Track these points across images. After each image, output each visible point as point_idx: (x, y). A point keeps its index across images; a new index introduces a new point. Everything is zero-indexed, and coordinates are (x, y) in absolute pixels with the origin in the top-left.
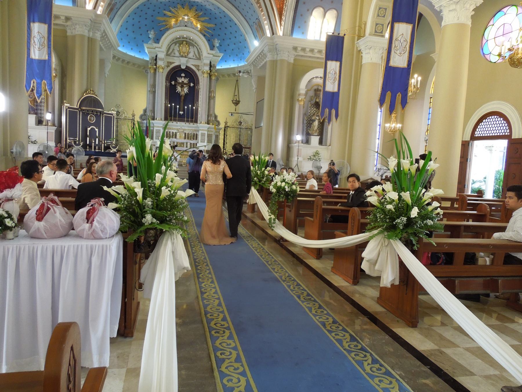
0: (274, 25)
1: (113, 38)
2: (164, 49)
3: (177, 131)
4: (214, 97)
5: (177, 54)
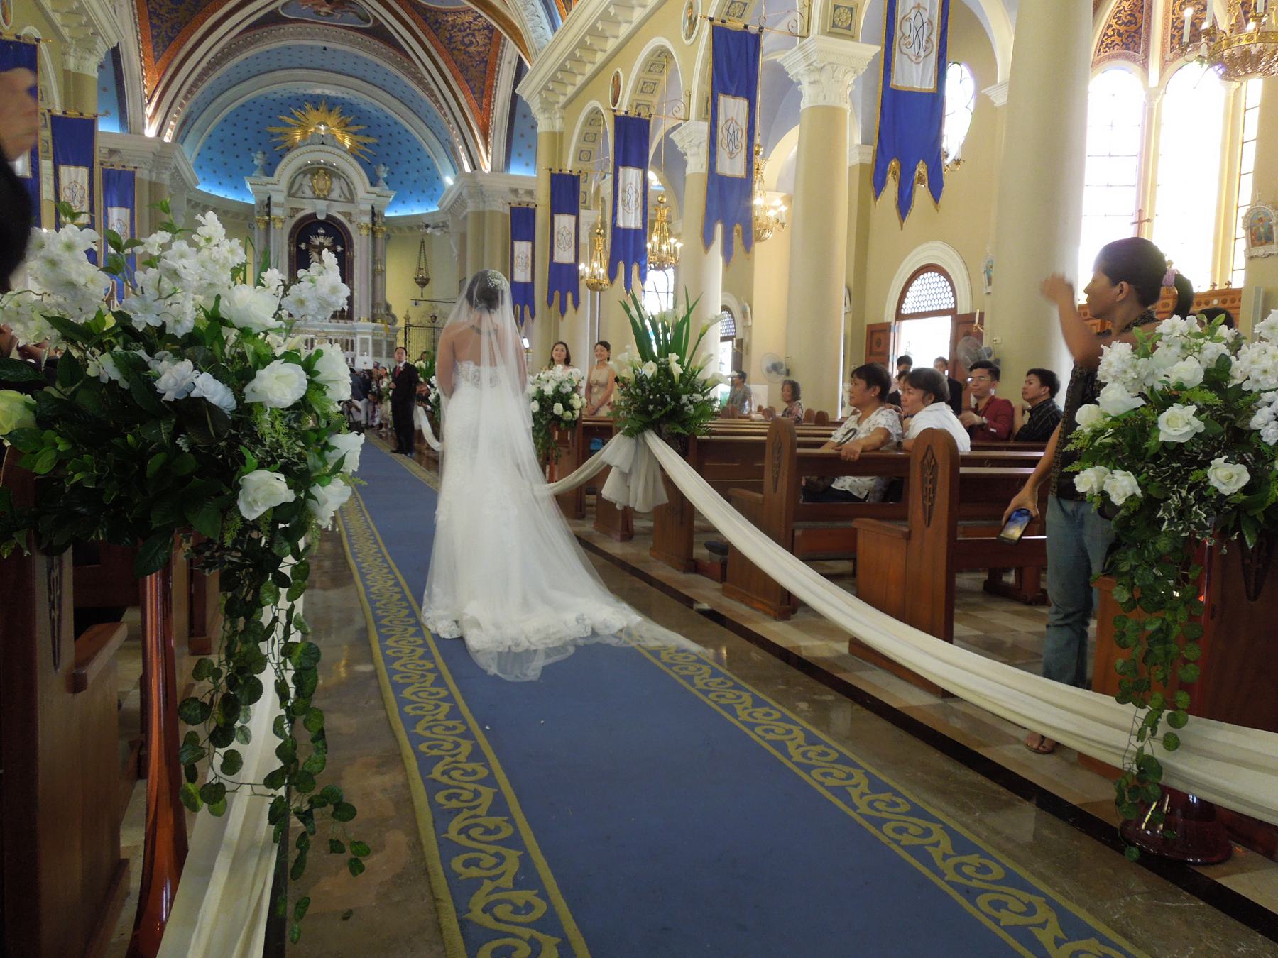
0: (475, 153)
1: (188, 174)
2: (283, 186)
3: (313, 336)
4: (383, 272)
5: (309, 193)
